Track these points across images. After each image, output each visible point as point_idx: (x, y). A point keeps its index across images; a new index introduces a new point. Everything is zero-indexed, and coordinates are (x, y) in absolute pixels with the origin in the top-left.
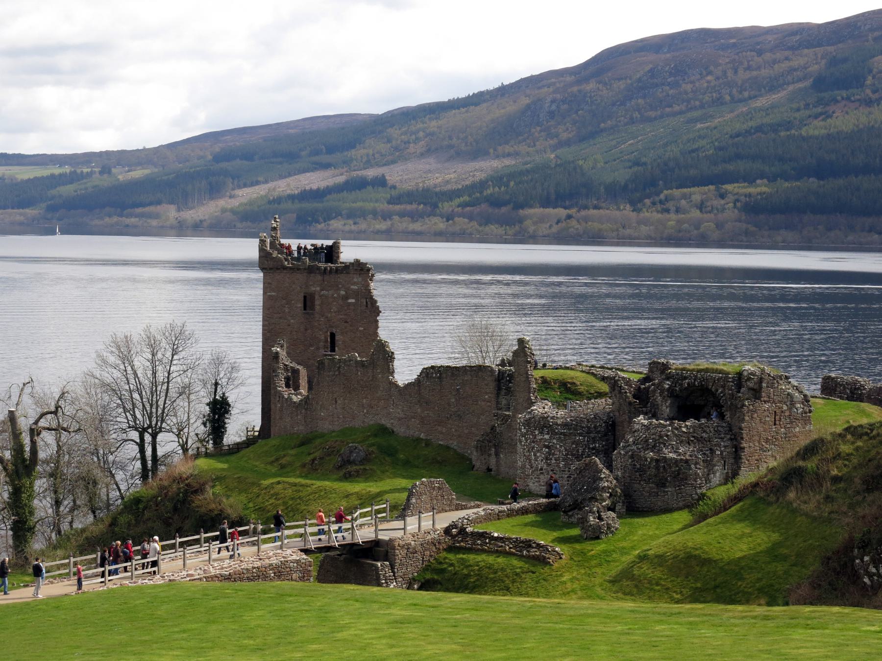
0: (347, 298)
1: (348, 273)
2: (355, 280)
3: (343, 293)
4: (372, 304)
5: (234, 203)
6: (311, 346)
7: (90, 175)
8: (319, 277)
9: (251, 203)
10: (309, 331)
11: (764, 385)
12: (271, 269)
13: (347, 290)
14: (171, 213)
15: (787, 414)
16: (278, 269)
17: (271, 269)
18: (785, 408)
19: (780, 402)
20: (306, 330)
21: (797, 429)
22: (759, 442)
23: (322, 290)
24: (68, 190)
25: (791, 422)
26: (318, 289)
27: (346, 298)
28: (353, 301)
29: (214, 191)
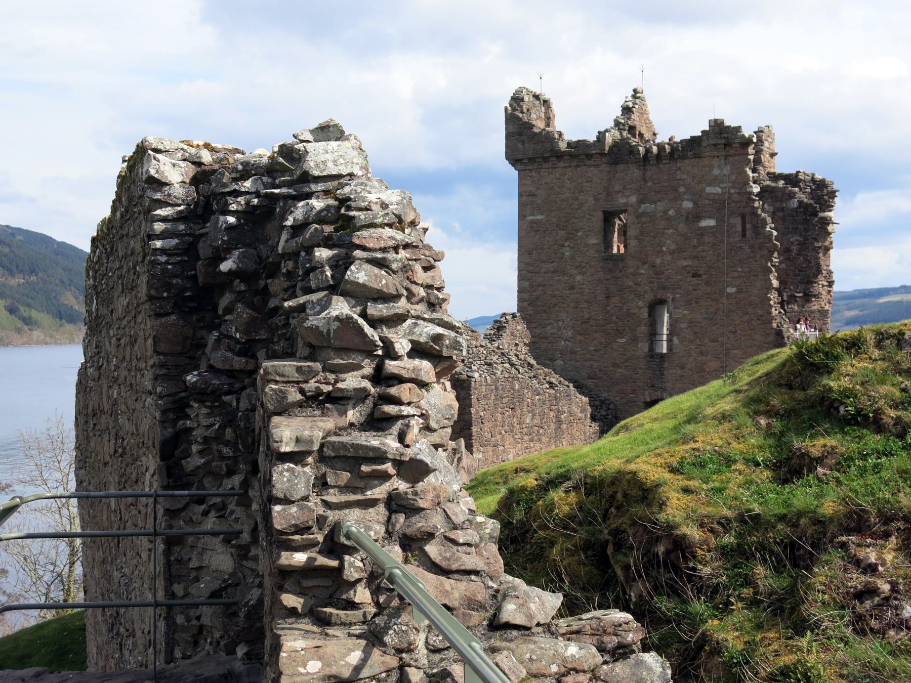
0: (698, 218)
1: (698, 156)
2: (716, 172)
3: (688, 205)
4: (755, 227)
6: (620, 334)
8: (635, 172)
10: (615, 300)
12: (531, 160)
13: (697, 197)
16: (546, 159)
17: (531, 160)
20: (608, 297)
23: (641, 202)
26: (633, 199)
28: (712, 223)
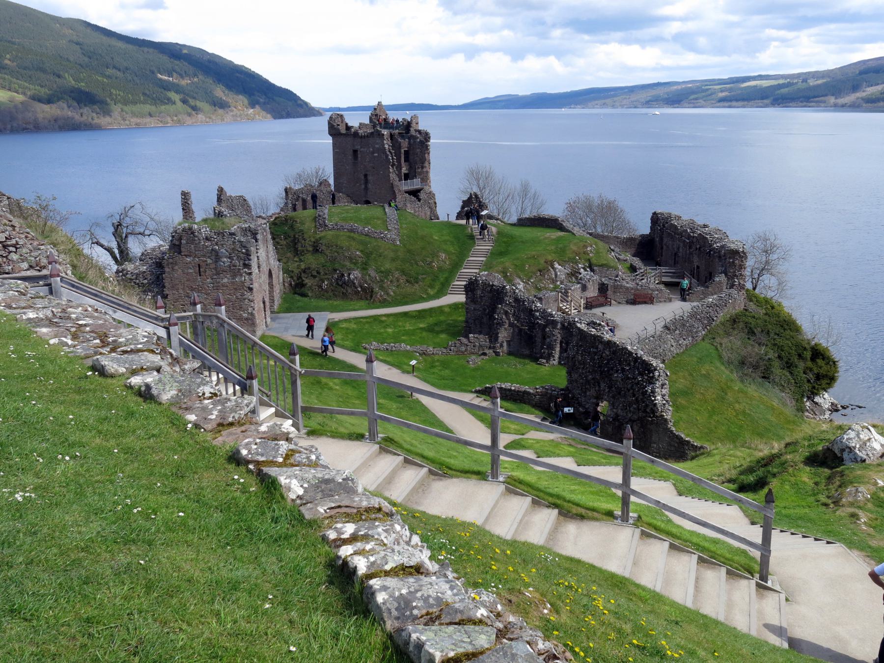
5: (864, 94)
7: (796, 83)
8: (359, 140)
9: (872, 94)
11: (183, 242)
14: (832, 100)
15: (213, 266)
18: (209, 261)
19: (204, 256)
21: (225, 280)
22: (183, 289)
24: (784, 91)
25: (218, 274)
27: (373, 153)
29: (855, 88)
